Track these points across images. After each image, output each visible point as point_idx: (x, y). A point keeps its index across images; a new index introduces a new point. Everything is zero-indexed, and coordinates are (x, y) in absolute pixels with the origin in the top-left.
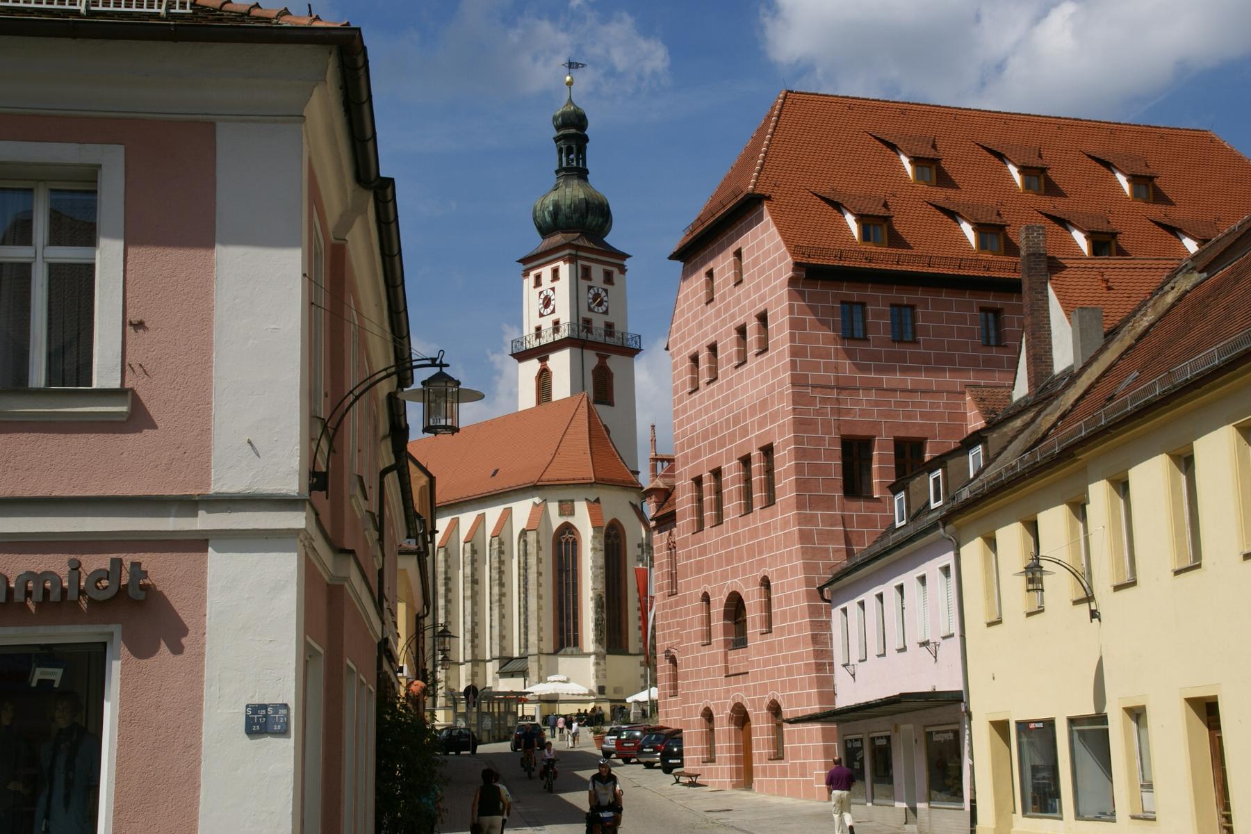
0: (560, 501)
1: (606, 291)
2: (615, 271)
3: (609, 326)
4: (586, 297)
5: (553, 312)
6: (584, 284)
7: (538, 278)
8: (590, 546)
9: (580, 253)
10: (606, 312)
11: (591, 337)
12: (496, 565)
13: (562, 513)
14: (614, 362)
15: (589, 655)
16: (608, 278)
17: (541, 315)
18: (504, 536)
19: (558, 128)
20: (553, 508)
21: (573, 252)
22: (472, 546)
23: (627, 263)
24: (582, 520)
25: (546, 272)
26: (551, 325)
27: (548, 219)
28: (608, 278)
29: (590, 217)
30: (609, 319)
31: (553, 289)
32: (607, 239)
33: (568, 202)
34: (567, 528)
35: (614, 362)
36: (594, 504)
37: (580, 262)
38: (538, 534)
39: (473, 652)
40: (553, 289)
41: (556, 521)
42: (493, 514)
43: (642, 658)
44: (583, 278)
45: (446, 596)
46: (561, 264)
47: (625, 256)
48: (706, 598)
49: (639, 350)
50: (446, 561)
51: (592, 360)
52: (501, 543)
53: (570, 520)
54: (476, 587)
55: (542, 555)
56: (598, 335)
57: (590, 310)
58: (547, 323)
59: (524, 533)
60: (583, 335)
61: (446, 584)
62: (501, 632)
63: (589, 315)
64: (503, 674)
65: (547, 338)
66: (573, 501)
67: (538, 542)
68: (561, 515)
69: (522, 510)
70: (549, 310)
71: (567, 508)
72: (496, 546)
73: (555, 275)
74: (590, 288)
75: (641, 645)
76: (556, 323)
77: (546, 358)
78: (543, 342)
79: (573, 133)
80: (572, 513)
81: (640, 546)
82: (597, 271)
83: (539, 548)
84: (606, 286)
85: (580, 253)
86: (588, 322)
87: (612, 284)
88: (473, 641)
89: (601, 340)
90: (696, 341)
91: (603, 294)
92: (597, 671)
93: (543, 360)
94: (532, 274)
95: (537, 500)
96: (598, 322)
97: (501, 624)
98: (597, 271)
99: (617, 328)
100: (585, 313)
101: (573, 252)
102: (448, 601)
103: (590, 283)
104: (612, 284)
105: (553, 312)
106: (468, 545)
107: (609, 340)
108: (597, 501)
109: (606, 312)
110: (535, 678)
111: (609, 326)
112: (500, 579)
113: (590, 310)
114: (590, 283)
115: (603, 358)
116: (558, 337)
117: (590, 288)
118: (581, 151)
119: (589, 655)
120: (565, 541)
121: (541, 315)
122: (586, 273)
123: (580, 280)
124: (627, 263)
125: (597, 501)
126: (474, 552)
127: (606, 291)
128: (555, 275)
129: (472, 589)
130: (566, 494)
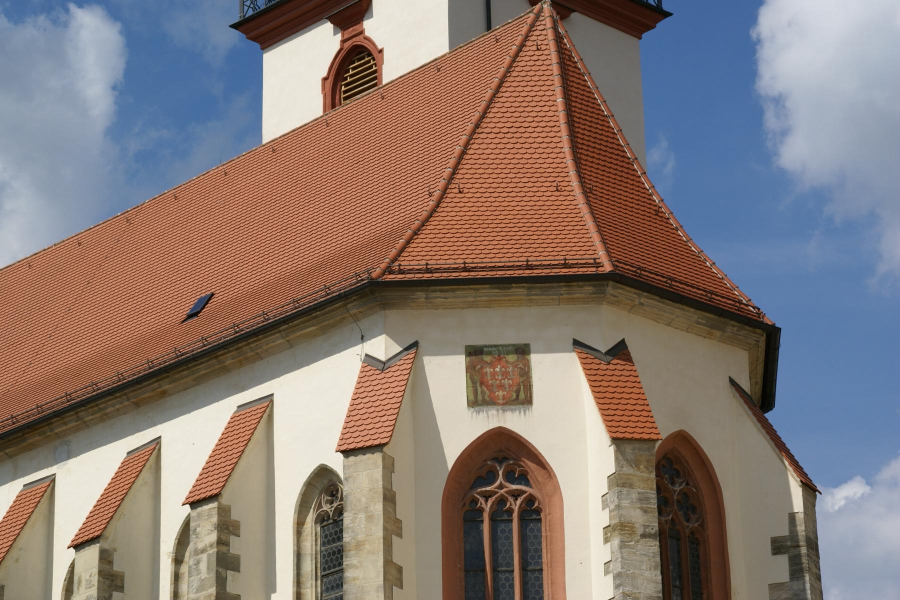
0: (473, 352)
8: (600, 518)
13: (480, 396)
18: (241, 497)
20: (446, 376)
22: (105, 558)
34: (504, 459)
36: (609, 364)
38: (389, 468)
41: (459, 426)
42: (188, 438)
52: (227, 528)
53: (514, 421)
55: (403, 553)
59: (323, 485)
66: (523, 351)
67: (389, 498)
68: (477, 402)
69: (312, 404)
71: (499, 376)
72: (206, 535)
80: (522, 396)
81: (778, 546)
83: (393, 528)
95: (381, 347)
106: (92, 553)
108: (620, 351)
125: (620, 351)
130: (498, 324)
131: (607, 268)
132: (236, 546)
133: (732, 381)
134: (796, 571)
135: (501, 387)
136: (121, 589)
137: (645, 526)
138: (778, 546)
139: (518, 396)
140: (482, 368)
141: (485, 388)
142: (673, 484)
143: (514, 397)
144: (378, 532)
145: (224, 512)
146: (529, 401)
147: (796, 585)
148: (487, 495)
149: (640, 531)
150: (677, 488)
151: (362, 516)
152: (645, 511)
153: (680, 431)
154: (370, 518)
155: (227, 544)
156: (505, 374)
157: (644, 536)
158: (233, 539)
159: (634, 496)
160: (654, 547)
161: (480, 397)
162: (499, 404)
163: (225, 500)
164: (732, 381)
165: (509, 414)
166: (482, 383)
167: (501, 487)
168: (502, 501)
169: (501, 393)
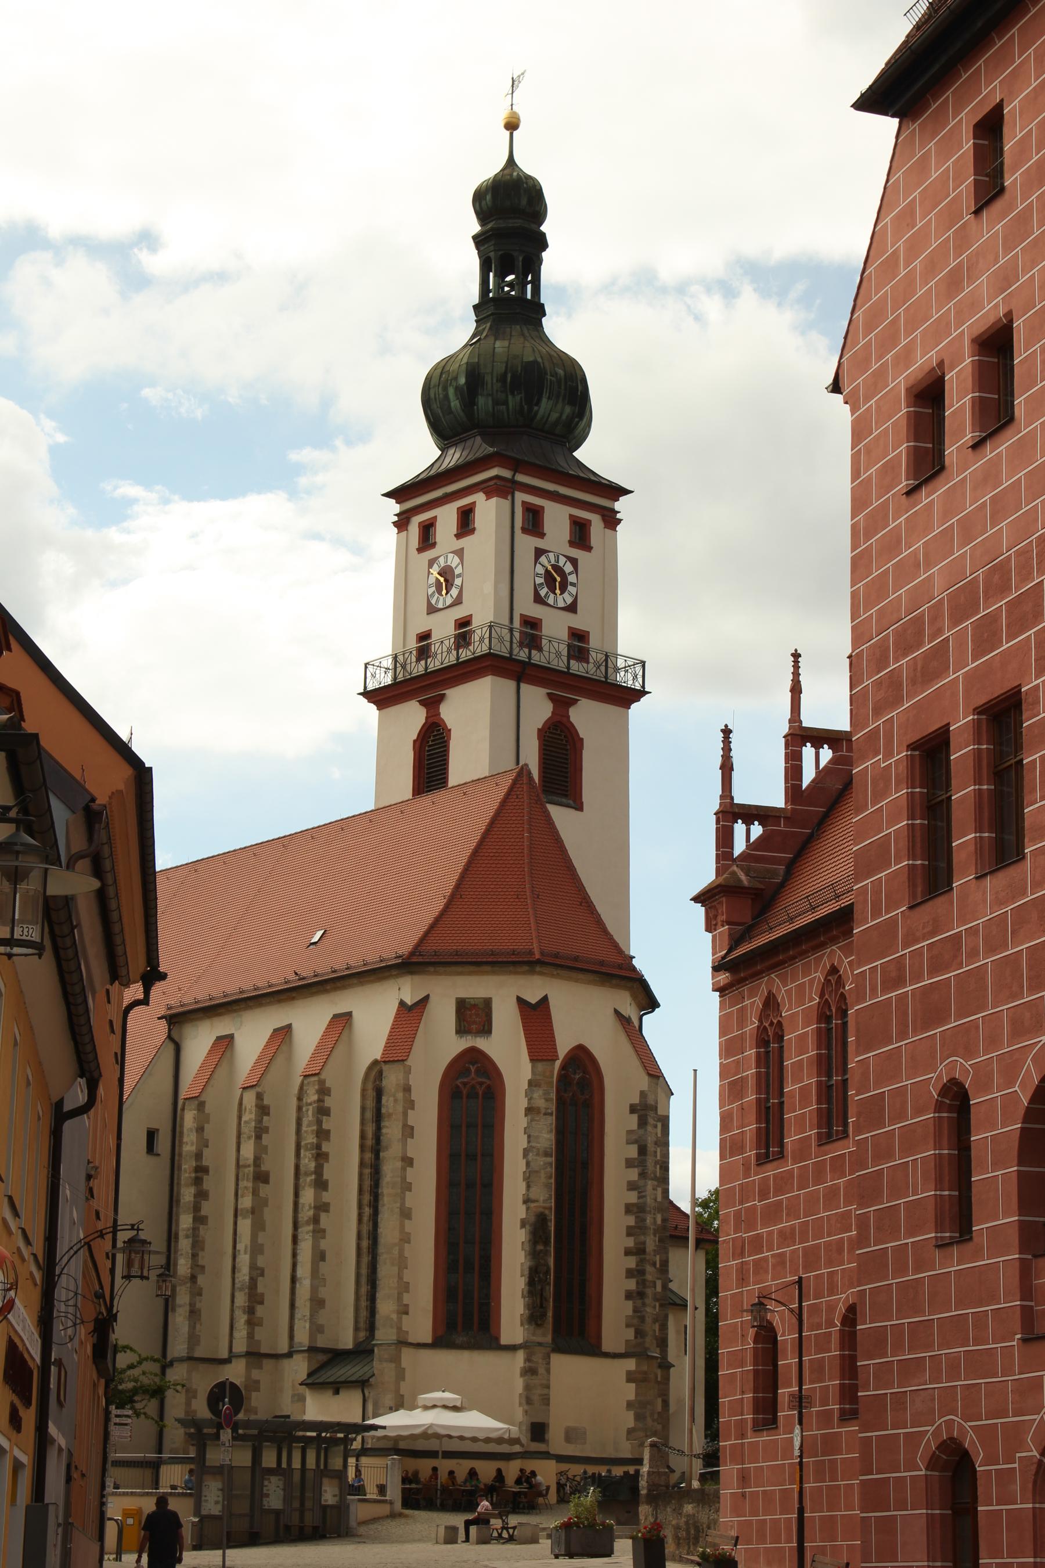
1: (574, 562)
2: (596, 522)
3: (578, 637)
4: (529, 575)
5: (458, 602)
6: (526, 544)
7: (427, 531)
9: (521, 478)
10: (572, 608)
11: (537, 657)
12: (310, 1139)
14: (586, 716)
15: (512, 1348)
16: (580, 535)
17: (432, 610)
19: (482, 215)
21: (506, 473)
22: (259, 1097)
23: (621, 505)
24: (506, 1047)
25: (447, 517)
26: (450, 630)
27: (455, 404)
28: (580, 535)
29: (545, 405)
30: (578, 621)
31: (460, 553)
32: (580, 454)
33: (500, 368)
35: (586, 716)
37: (520, 497)
39: (250, 1336)
43: (631, 1364)
44: (524, 530)
45: (197, 1208)
46: (479, 498)
47: (618, 492)
48: (956, 1100)
49: (642, 693)
50: (200, 1130)
51: (538, 706)
53: (481, 1043)
54: (264, 1190)
56: (553, 653)
57: (538, 599)
58: (443, 628)
59: (376, 1071)
60: (522, 655)
61: (198, 1181)
62: (314, 1289)
63: (535, 611)
64: (315, 1382)
65: (443, 656)
72: (312, 1097)
73: (466, 523)
74: (539, 553)
75: (630, 1334)
76: (464, 623)
77: (442, 698)
78: (434, 664)
79: (511, 219)
80: (486, 1029)
82: (557, 519)
84: (575, 553)
85: (521, 478)
86: (532, 624)
87: (588, 548)
88: (251, 1311)
89: (560, 664)
90: (941, 329)
91: (568, 568)
92: (527, 1388)
93: (432, 705)
94: (416, 520)
96: (555, 627)
97: (315, 1272)
98: (557, 519)
99: (594, 642)
100: (525, 606)
101: (506, 473)
102: (200, 1220)
103: (541, 543)
104: (588, 548)
105: (458, 602)
107: (576, 667)
109: (572, 608)
110: (388, 1400)
111: (578, 637)
112: (319, 1171)
113: (538, 599)
114: (541, 543)
115: (561, 705)
116: (465, 654)
117: (539, 553)
118: (531, 265)
119: (512, 1348)
120: (471, 1089)
121: (432, 610)
122: (534, 521)
123: (521, 539)
124: (621, 505)
126: (263, 1110)
127: (574, 562)
128: (466, 523)
129: (255, 1192)
130: (474, 987)
131: (537, 956)
132: (328, 1102)
133: (616, 1012)
134: (643, 1123)
135: (474, 1022)
136: (268, 1114)
138: (633, 1109)
142: (575, 1073)
144: (400, 1108)
145: (322, 1082)
147: (641, 1132)
148: (465, 1084)
149: (543, 1111)
150: (577, 1077)
151: (391, 1099)
154: (396, 1101)
155: (323, 1101)
157: (545, 1114)
158: (326, 1098)
159: (541, 1092)
160: (552, 1120)
163: (323, 1077)
164: (616, 1012)
165: (478, 1039)
168: (473, 1087)
169: (474, 1027)
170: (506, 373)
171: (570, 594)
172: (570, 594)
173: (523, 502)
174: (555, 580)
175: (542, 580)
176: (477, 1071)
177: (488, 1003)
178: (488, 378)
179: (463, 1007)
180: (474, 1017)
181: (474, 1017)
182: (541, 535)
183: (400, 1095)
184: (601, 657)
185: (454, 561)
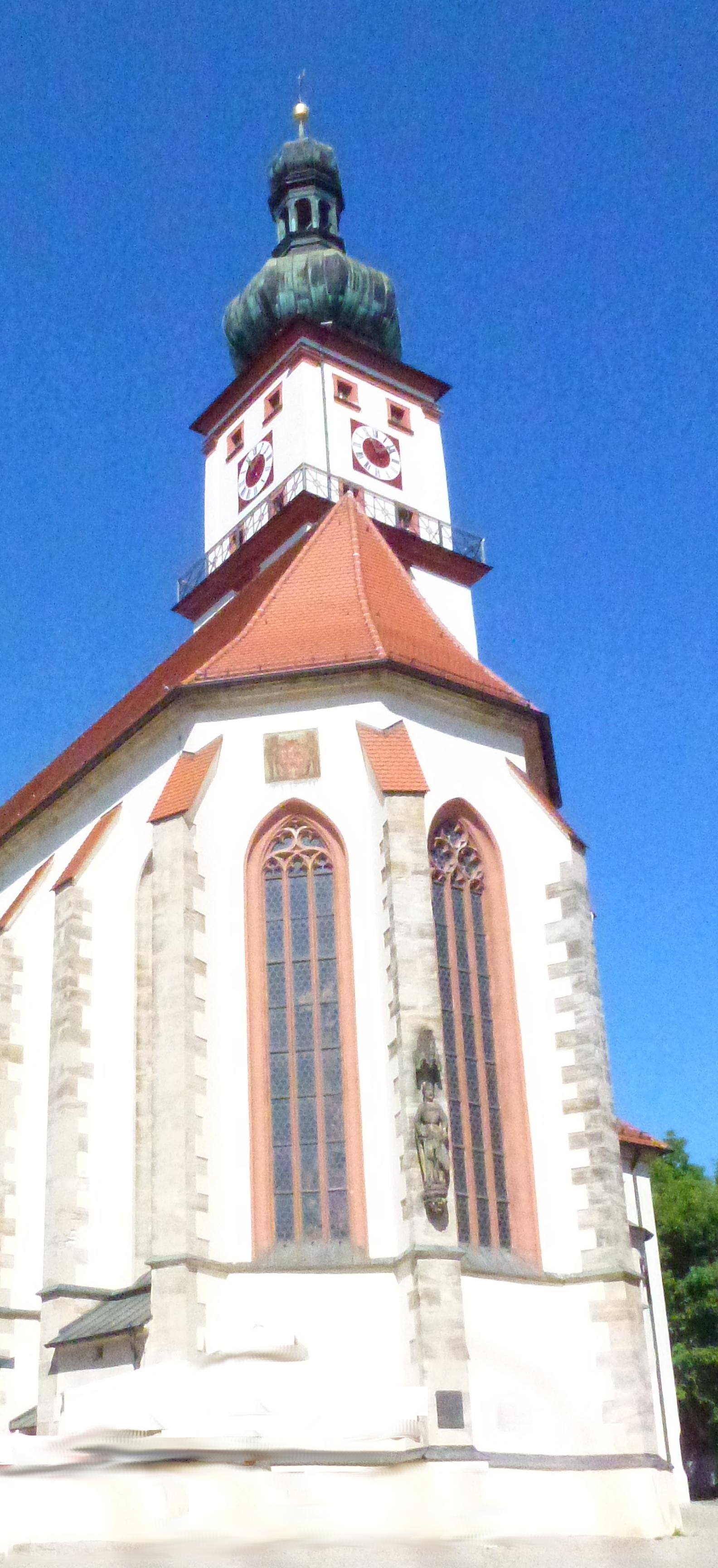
2: (415, 413)
4: (345, 448)
5: (270, 479)
10: (397, 483)
24: (343, 792)
30: (407, 497)
40: (269, 438)
63: (356, 478)
70: (260, 485)
74: (355, 425)
80: (311, 769)
87: (410, 432)
104: (410, 432)
113: (357, 466)
117: (355, 425)
127: (396, 442)
135: (293, 764)
136: (21, 968)
137: (416, 865)
139: (308, 771)
140: (278, 750)
141: (280, 768)
143: (305, 771)
144: (180, 883)
146: (317, 774)
148: (285, 856)
151: (167, 873)
152: (416, 852)
153: (458, 799)
154: (173, 874)
156: (297, 754)
161: (275, 774)
162: (292, 779)
166: (277, 763)
167: (296, 847)
169: (293, 770)
170: (306, 269)
171: (393, 469)
172: (393, 469)
173: (334, 375)
174: (377, 454)
175: (361, 450)
176: (303, 834)
177: (311, 738)
178: (288, 275)
179: (274, 747)
180: (291, 758)
181: (291, 758)
182: (358, 409)
183: (180, 865)
184: (434, 527)
185: (264, 449)
